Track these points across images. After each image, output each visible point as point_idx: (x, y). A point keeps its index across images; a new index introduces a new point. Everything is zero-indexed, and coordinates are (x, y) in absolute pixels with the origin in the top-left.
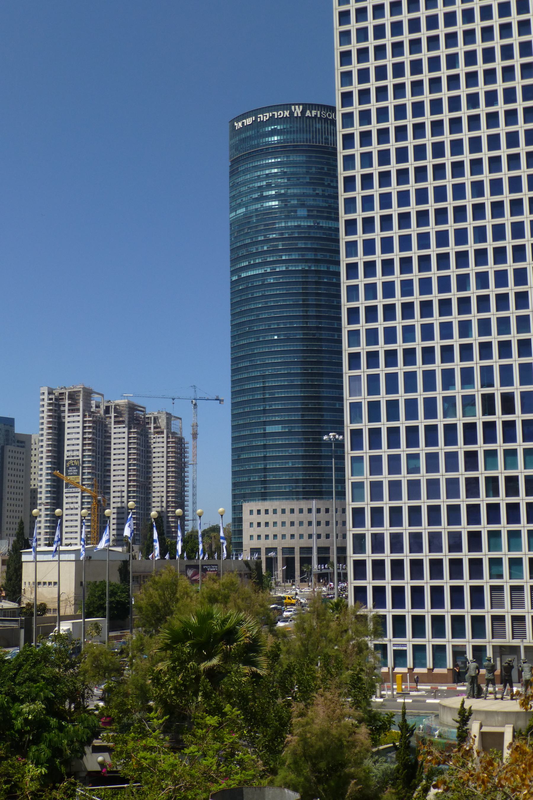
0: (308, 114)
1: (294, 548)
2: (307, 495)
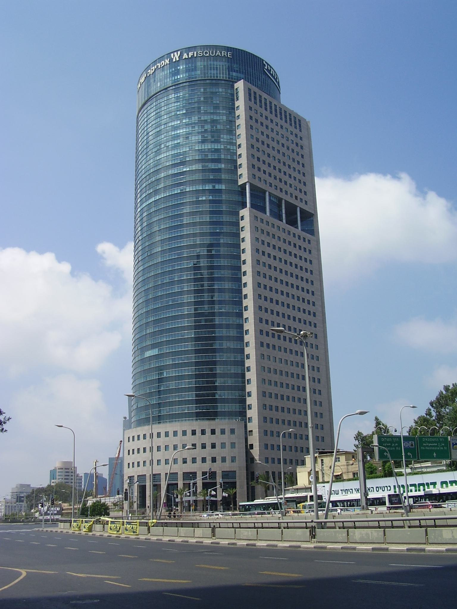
0: (185, 56)
1: (195, 473)
2: (199, 416)
